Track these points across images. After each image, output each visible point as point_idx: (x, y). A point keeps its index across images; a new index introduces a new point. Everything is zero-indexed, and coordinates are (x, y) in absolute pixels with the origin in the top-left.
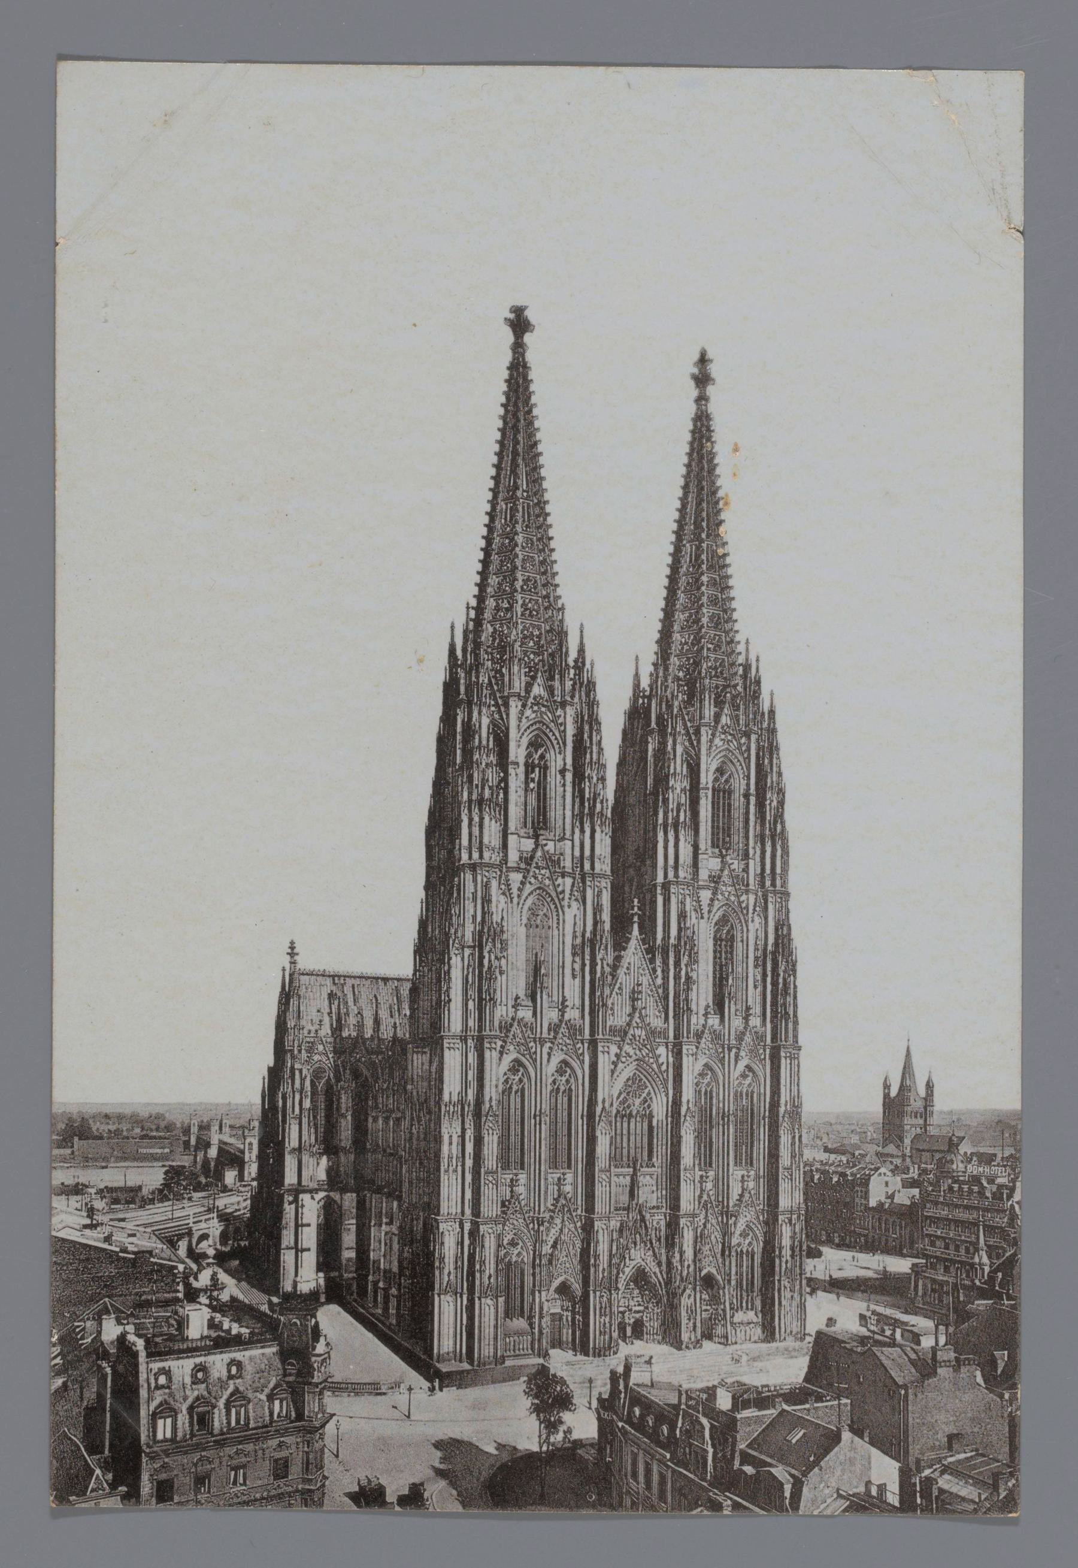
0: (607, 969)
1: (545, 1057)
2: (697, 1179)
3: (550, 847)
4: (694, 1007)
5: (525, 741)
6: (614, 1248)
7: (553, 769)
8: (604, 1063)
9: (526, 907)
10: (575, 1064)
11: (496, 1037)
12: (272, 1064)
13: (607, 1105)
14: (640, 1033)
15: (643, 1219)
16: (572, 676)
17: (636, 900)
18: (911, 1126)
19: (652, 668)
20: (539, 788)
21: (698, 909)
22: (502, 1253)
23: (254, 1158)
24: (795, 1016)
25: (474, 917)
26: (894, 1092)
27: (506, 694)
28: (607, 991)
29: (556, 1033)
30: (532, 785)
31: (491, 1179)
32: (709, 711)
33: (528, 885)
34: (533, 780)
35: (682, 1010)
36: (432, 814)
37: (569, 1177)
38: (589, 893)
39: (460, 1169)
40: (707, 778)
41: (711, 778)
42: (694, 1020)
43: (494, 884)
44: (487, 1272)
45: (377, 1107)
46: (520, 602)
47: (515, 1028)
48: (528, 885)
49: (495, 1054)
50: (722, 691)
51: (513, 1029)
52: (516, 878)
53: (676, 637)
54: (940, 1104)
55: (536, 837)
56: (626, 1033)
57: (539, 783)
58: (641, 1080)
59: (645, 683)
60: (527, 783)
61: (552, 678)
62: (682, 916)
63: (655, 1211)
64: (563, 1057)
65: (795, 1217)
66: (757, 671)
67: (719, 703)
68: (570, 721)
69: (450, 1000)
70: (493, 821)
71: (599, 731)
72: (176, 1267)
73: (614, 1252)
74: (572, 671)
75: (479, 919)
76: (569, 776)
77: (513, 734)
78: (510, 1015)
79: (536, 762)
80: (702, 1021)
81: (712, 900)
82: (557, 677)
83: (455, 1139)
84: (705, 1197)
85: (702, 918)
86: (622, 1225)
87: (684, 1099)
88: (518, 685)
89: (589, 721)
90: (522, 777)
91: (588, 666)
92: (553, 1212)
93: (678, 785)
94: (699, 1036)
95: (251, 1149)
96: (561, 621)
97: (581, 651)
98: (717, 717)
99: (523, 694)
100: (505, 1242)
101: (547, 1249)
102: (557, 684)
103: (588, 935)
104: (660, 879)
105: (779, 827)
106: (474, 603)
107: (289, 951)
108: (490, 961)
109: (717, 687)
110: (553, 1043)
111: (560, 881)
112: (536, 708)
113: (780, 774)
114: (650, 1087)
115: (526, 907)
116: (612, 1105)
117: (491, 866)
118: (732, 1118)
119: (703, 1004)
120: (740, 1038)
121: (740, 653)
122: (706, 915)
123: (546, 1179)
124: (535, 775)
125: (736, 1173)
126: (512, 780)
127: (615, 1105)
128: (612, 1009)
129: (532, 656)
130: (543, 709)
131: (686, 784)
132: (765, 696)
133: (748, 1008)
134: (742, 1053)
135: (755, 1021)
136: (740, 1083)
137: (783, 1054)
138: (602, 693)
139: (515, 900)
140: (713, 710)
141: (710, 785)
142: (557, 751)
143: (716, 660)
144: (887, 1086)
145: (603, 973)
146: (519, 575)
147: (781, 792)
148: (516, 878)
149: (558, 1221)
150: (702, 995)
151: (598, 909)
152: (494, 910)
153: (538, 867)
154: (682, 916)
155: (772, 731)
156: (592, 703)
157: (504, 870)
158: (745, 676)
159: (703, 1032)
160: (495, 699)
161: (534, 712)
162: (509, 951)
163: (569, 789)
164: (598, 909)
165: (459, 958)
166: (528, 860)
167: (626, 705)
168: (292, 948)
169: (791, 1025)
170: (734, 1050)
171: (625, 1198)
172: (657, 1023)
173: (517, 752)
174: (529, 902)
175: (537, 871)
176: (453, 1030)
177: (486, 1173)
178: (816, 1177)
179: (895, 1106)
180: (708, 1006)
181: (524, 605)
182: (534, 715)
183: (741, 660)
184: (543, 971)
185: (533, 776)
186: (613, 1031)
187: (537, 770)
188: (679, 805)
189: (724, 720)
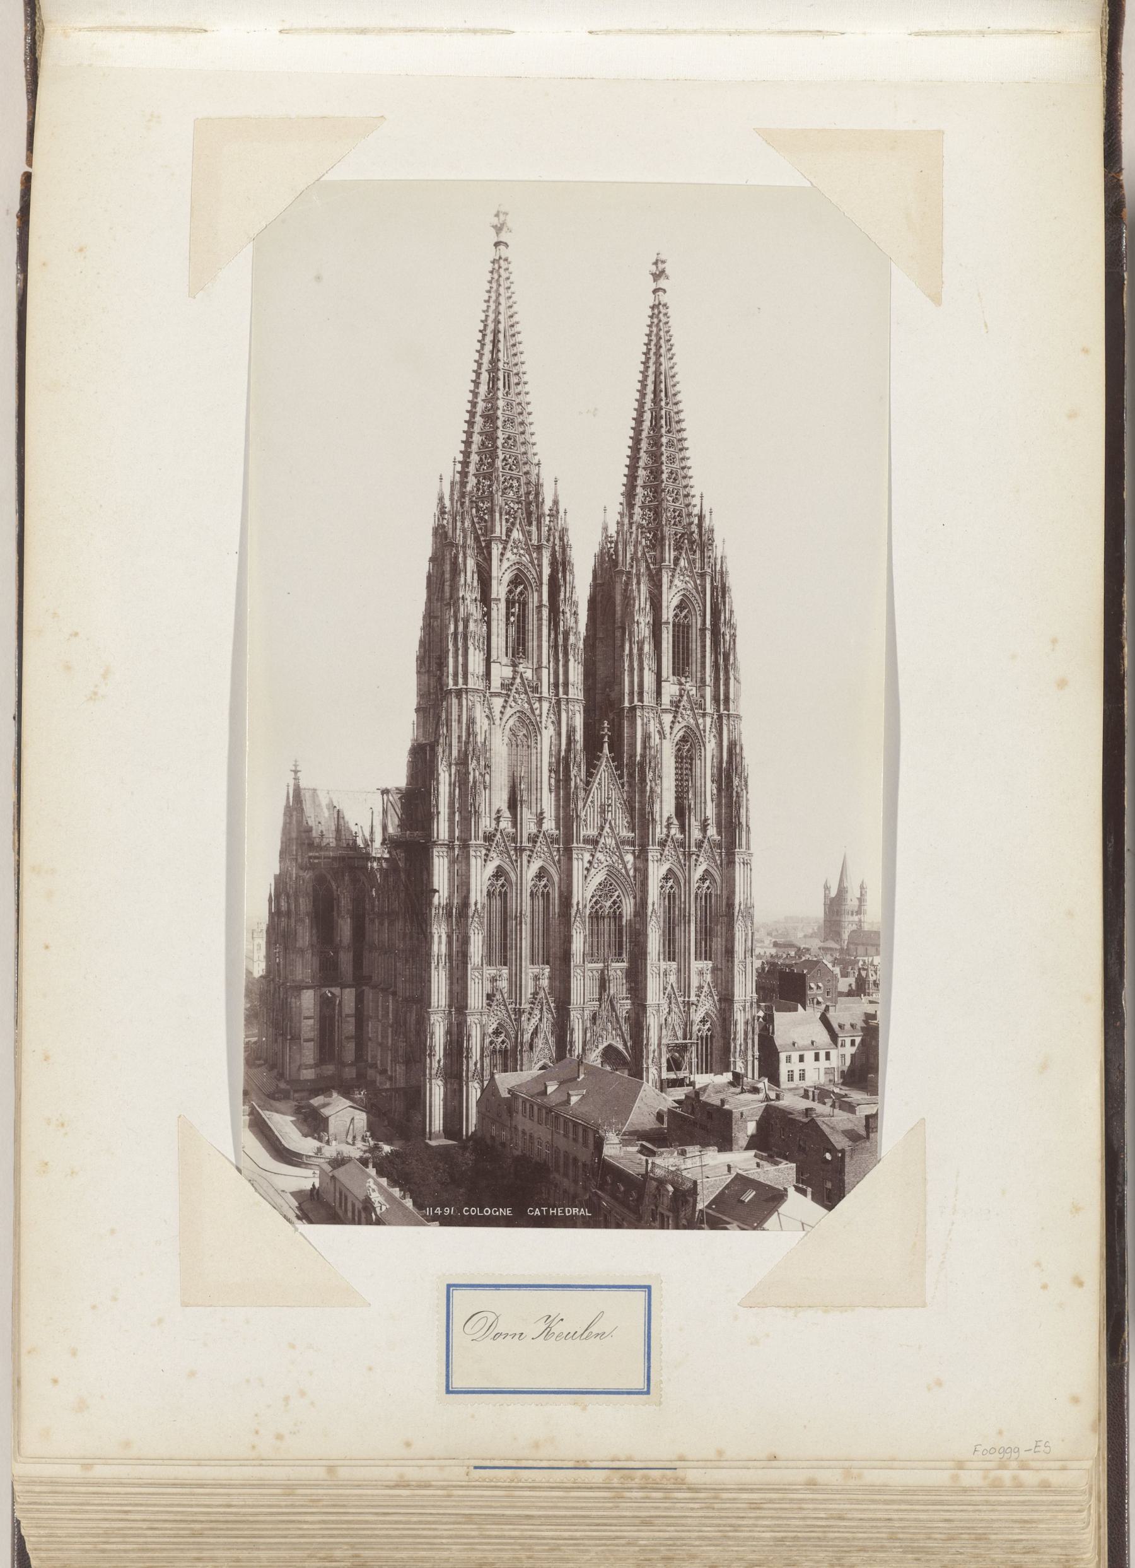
0: (581, 785)
1: (525, 862)
4: (658, 818)
6: (588, 1035)
7: (530, 605)
8: (578, 868)
9: (508, 728)
11: (480, 846)
14: (610, 842)
15: (613, 1009)
19: (618, 517)
20: (518, 621)
22: (487, 1041)
24: (747, 826)
25: (460, 737)
28: (580, 804)
29: (536, 842)
30: (512, 619)
33: (508, 708)
34: (513, 614)
36: (422, 643)
37: (547, 970)
40: (668, 614)
41: (672, 614)
42: (658, 830)
43: (478, 707)
46: (501, 457)
51: (496, 838)
53: (639, 490)
56: (597, 842)
57: (519, 616)
59: (612, 531)
60: (508, 619)
61: (530, 524)
62: (647, 737)
65: (748, 1004)
67: (678, 548)
68: (546, 562)
71: (572, 572)
74: (548, 518)
76: (545, 612)
80: (665, 830)
81: (673, 722)
82: (534, 523)
87: (650, 901)
89: (561, 565)
92: (533, 1003)
94: (663, 844)
96: (538, 475)
97: (556, 502)
99: (504, 538)
100: (491, 1031)
101: (527, 1037)
102: (534, 528)
103: (563, 753)
104: (627, 704)
105: (732, 658)
106: (460, 457)
108: (474, 777)
109: (676, 534)
110: (532, 851)
113: (731, 612)
115: (508, 728)
118: (693, 918)
119: (666, 815)
121: (695, 506)
122: (668, 736)
125: (696, 965)
126: (494, 614)
127: (588, 906)
130: (522, 552)
131: (649, 619)
132: (718, 541)
133: (706, 820)
134: (701, 859)
135: (712, 831)
136: (699, 888)
137: (737, 860)
138: (572, 538)
139: (498, 722)
141: (671, 620)
143: (674, 511)
145: (576, 788)
146: (500, 433)
147: (733, 627)
148: (497, 703)
149: (537, 1012)
150: (666, 806)
151: (571, 731)
152: (478, 730)
153: (517, 692)
158: (700, 526)
159: (666, 841)
162: (493, 768)
163: (545, 623)
164: (571, 731)
165: (447, 774)
166: (507, 686)
167: (597, 550)
169: (744, 834)
170: (694, 857)
172: (625, 833)
173: (499, 590)
174: (511, 722)
176: (441, 837)
181: (505, 459)
183: (696, 511)
186: (587, 841)
189: (683, 563)
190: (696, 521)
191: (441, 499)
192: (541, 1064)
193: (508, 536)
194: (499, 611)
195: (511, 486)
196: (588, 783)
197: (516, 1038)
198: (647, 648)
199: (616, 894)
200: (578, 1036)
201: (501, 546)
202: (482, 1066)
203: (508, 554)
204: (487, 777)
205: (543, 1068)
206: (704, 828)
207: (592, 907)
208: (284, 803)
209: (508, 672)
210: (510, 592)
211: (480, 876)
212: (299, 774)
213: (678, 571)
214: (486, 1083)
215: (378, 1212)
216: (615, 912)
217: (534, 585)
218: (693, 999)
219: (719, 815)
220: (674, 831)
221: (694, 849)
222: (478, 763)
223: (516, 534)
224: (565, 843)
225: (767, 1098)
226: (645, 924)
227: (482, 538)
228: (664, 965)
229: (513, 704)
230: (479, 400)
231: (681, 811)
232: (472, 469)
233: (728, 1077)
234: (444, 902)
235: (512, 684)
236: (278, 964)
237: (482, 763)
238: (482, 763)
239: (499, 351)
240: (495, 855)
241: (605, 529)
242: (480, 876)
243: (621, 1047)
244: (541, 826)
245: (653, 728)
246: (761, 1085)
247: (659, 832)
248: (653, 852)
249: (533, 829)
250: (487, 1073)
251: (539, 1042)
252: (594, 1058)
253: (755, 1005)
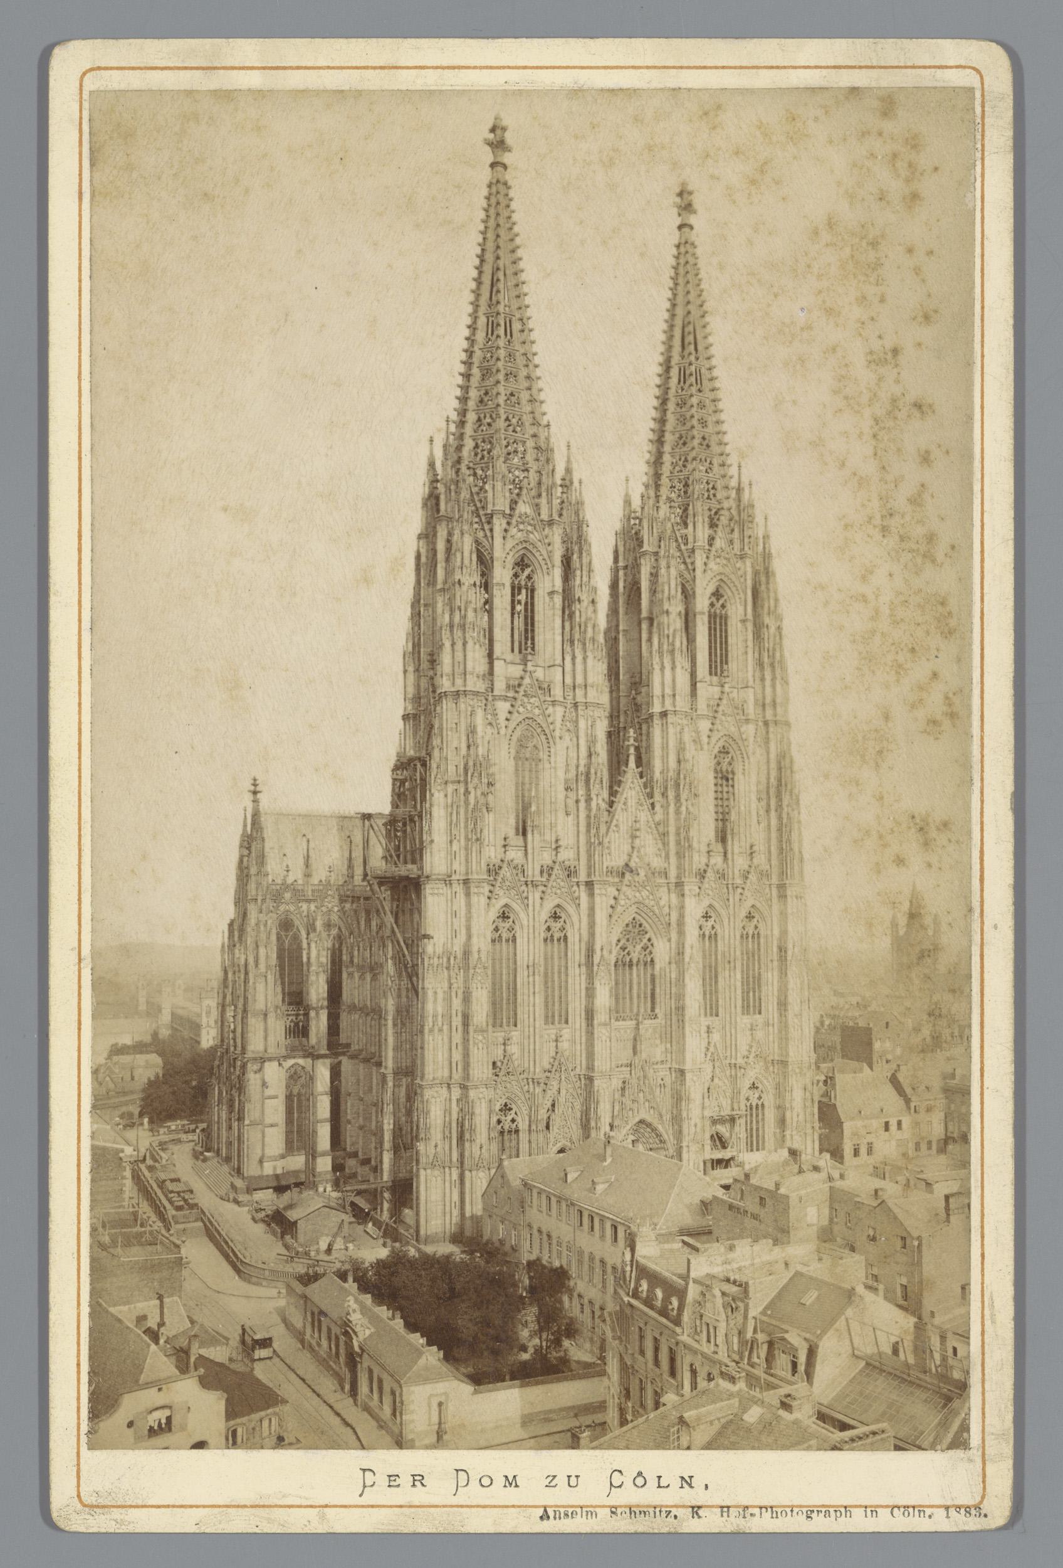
0: (604, 806)
1: (538, 901)
2: (704, 1029)
3: (540, 674)
4: (695, 845)
5: (511, 560)
9: (514, 738)
10: (571, 909)
16: (559, 494)
17: (631, 731)
20: (526, 610)
21: (696, 741)
23: (212, 1023)
27: (489, 511)
30: (519, 608)
31: (480, 1038)
32: (702, 532)
33: (516, 714)
34: (519, 602)
35: (684, 848)
38: (582, 724)
39: (445, 1028)
40: (702, 603)
41: (707, 603)
42: (696, 857)
43: (480, 713)
44: (478, 1141)
46: (503, 417)
47: (506, 872)
48: (516, 714)
49: (483, 900)
50: (716, 513)
51: (502, 872)
52: (503, 707)
55: (525, 662)
57: (526, 604)
58: (640, 925)
59: (636, 502)
60: (513, 608)
62: (681, 749)
63: (659, 1066)
64: (557, 901)
66: (750, 493)
69: (432, 841)
70: (477, 646)
72: (122, 1151)
73: (616, 1113)
74: (560, 489)
77: (498, 553)
78: (499, 857)
79: (523, 583)
82: (544, 494)
83: (440, 995)
84: (712, 1049)
85: (702, 749)
86: (624, 1082)
88: (502, 504)
90: (509, 598)
91: (576, 483)
93: (676, 607)
94: (702, 875)
95: (208, 1013)
96: (547, 439)
97: (568, 471)
98: (711, 540)
99: (508, 511)
100: (498, 1107)
101: (543, 1114)
103: (582, 769)
105: (778, 655)
106: (454, 416)
107: (252, 788)
108: (476, 798)
111: (550, 710)
112: (521, 527)
113: (776, 600)
115: (514, 738)
116: (610, 952)
117: (476, 694)
120: (745, 876)
122: (706, 747)
123: (541, 1037)
124: (522, 597)
126: (497, 602)
128: (608, 848)
129: (517, 473)
132: (759, 519)
139: (503, 731)
140: (708, 531)
141: (706, 610)
142: (545, 571)
145: (599, 809)
148: (503, 707)
149: (555, 1083)
150: (705, 829)
151: (592, 741)
152: (479, 741)
154: (681, 749)
155: (767, 556)
156: (580, 524)
157: (490, 698)
160: (478, 516)
161: (520, 530)
165: (442, 794)
166: (515, 686)
171: (626, 1055)
172: (657, 863)
173: (502, 575)
174: (518, 733)
175: (526, 700)
177: (475, 1031)
178: (827, 1023)
181: (507, 419)
182: (520, 534)
183: (733, 483)
184: (533, 808)
185: (519, 597)
186: (610, 872)
187: (524, 591)
188: (675, 631)
189: (719, 543)
190: (733, 494)
191: (432, 465)
192: (559, 1146)
193: (512, 509)
194: (502, 599)
195: (516, 452)
196: (611, 804)
198: (680, 641)
199: (647, 936)
201: (504, 522)
203: (513, 531)
205: (561, 1151)
209: (516, 671)
210: (516, 575)
212: (259, 795)
213: (713, 552)
217: (545, 567)
218: (740, 1061)
220: (717, 860)
221: (739, 881)
223: (523, 508)
225: (830, 1179)
227: (481, 512)
228: (705, 1021)
229: (521, 709)
230: (476, 348)
231: (722, 837)
232: (469, 429)
235: (519, 685)
238: (485, 780)
239: (498, 291)
240: (501, 893)
241: (628, 502)
243: (656, 1123)
245: (687, 737)
246: (821, 1163)
247: (699, 860)
248: (691, 887)
249: (547, 858)
252: (622, 1136)
253: (813, 1067)
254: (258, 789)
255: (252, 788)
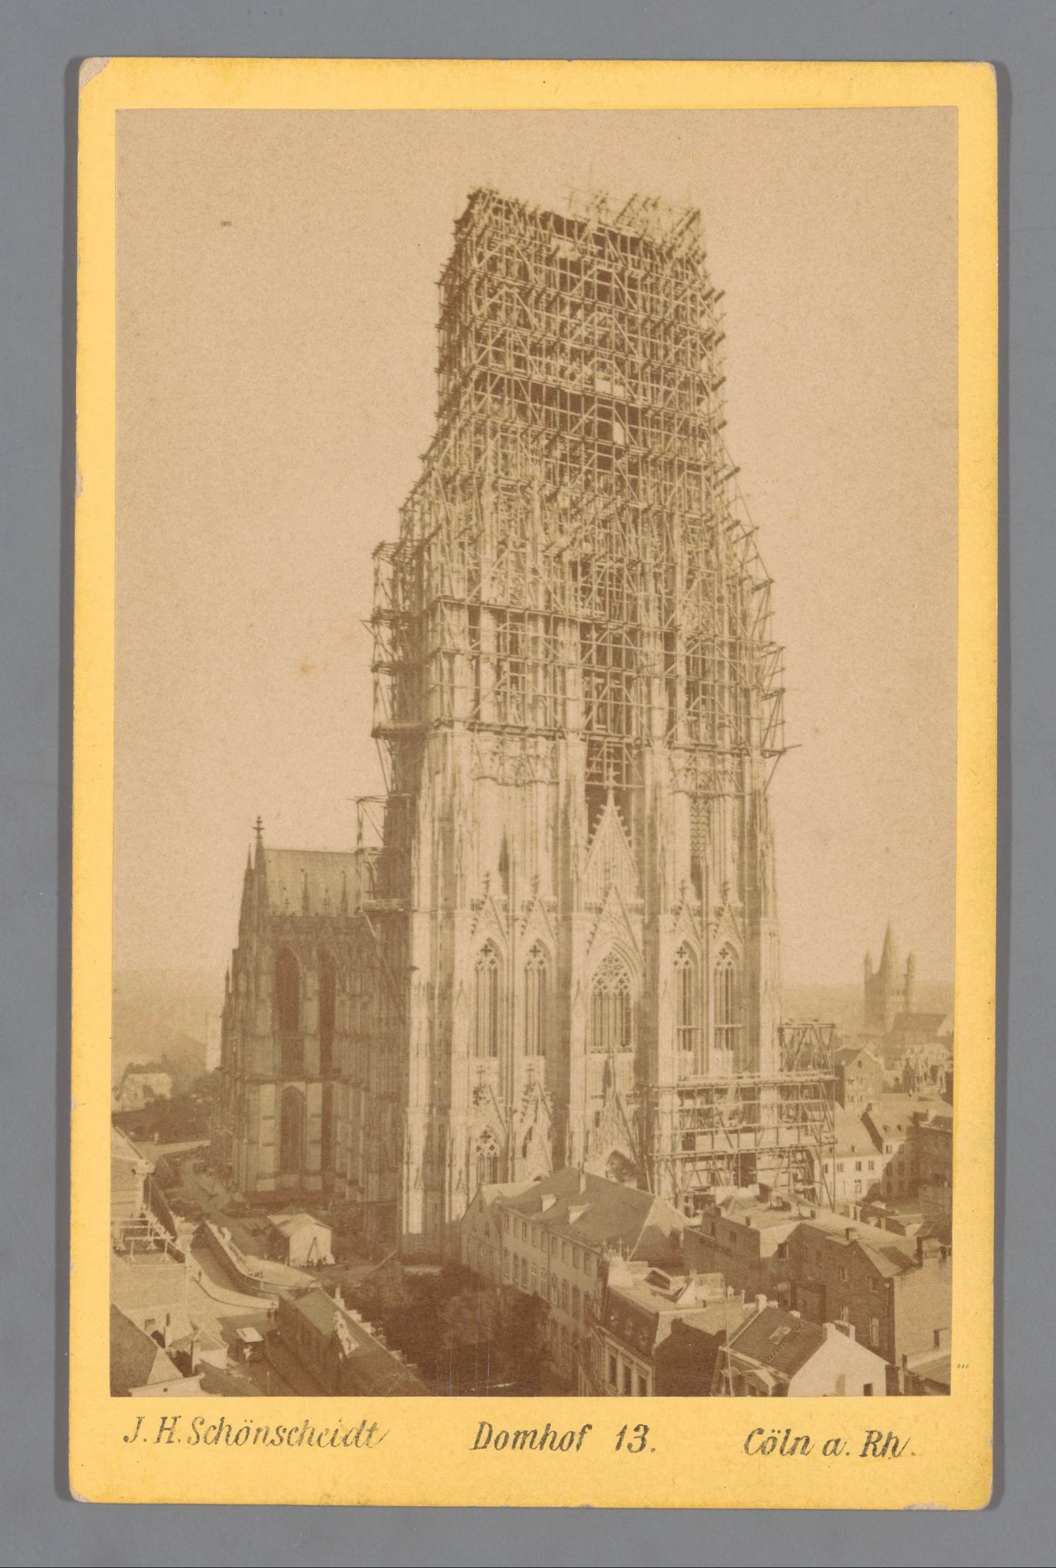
6: (591, 1138)
8: (579, 939)
12: (236, 945)
13: (582, 987)
14: (616, 910)
18: (894, 1005)
24: (774, 890)
25: (444, 789)
26: (875, 970)
42: (671, 896)
45: (344, 990)
47: (487, 906)
54: (920, 977)
75: (448, 792)
80: (679, 896)
94: (677, 912)
101: (519, 1142)
114: (626, 967)
119: (679, 879)
134: (721, 930)
135: (733, 897)
136: (718, 964)
144: (867, 962)
145: (577, 846)
149: (530, 1111)
150: (678, 869)
168: (259, 822)
176: (422, 905)
179: (877, 984)
180: (683, 881)
197: (507, 1143)
200: (578, 1143)
202: (468, 1175)
204: (475, 835)
206: (724, 893)
207: (595, 988)
208: (245, 867)
211: (466, 953)
212: (262, 832)
214: (472, 1196)
215: (347, 1352)
216: (621, 994)
219: (741, 878)
222: (465, 818)
224: (565, 911)
226: (656, 1006)
231: (696, 874)
233: (753, 1191)
234: (424, 982)
236: (235, 1054)
237: (470, 818)
238: (470, 818)
242: (466, 953)
244: (536, 891)
248: (665, 920)
250: (473, 1185)
251: (532, 1146)
254: (262, 825)
255: (256, 825)
